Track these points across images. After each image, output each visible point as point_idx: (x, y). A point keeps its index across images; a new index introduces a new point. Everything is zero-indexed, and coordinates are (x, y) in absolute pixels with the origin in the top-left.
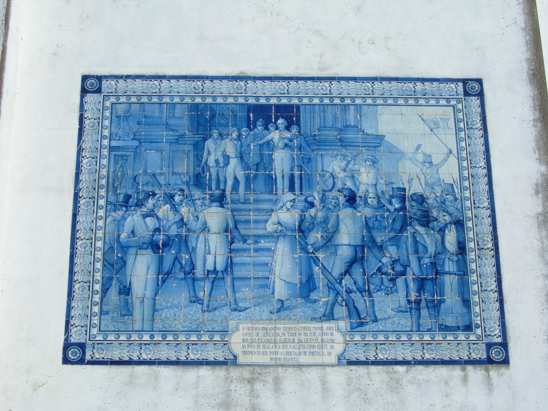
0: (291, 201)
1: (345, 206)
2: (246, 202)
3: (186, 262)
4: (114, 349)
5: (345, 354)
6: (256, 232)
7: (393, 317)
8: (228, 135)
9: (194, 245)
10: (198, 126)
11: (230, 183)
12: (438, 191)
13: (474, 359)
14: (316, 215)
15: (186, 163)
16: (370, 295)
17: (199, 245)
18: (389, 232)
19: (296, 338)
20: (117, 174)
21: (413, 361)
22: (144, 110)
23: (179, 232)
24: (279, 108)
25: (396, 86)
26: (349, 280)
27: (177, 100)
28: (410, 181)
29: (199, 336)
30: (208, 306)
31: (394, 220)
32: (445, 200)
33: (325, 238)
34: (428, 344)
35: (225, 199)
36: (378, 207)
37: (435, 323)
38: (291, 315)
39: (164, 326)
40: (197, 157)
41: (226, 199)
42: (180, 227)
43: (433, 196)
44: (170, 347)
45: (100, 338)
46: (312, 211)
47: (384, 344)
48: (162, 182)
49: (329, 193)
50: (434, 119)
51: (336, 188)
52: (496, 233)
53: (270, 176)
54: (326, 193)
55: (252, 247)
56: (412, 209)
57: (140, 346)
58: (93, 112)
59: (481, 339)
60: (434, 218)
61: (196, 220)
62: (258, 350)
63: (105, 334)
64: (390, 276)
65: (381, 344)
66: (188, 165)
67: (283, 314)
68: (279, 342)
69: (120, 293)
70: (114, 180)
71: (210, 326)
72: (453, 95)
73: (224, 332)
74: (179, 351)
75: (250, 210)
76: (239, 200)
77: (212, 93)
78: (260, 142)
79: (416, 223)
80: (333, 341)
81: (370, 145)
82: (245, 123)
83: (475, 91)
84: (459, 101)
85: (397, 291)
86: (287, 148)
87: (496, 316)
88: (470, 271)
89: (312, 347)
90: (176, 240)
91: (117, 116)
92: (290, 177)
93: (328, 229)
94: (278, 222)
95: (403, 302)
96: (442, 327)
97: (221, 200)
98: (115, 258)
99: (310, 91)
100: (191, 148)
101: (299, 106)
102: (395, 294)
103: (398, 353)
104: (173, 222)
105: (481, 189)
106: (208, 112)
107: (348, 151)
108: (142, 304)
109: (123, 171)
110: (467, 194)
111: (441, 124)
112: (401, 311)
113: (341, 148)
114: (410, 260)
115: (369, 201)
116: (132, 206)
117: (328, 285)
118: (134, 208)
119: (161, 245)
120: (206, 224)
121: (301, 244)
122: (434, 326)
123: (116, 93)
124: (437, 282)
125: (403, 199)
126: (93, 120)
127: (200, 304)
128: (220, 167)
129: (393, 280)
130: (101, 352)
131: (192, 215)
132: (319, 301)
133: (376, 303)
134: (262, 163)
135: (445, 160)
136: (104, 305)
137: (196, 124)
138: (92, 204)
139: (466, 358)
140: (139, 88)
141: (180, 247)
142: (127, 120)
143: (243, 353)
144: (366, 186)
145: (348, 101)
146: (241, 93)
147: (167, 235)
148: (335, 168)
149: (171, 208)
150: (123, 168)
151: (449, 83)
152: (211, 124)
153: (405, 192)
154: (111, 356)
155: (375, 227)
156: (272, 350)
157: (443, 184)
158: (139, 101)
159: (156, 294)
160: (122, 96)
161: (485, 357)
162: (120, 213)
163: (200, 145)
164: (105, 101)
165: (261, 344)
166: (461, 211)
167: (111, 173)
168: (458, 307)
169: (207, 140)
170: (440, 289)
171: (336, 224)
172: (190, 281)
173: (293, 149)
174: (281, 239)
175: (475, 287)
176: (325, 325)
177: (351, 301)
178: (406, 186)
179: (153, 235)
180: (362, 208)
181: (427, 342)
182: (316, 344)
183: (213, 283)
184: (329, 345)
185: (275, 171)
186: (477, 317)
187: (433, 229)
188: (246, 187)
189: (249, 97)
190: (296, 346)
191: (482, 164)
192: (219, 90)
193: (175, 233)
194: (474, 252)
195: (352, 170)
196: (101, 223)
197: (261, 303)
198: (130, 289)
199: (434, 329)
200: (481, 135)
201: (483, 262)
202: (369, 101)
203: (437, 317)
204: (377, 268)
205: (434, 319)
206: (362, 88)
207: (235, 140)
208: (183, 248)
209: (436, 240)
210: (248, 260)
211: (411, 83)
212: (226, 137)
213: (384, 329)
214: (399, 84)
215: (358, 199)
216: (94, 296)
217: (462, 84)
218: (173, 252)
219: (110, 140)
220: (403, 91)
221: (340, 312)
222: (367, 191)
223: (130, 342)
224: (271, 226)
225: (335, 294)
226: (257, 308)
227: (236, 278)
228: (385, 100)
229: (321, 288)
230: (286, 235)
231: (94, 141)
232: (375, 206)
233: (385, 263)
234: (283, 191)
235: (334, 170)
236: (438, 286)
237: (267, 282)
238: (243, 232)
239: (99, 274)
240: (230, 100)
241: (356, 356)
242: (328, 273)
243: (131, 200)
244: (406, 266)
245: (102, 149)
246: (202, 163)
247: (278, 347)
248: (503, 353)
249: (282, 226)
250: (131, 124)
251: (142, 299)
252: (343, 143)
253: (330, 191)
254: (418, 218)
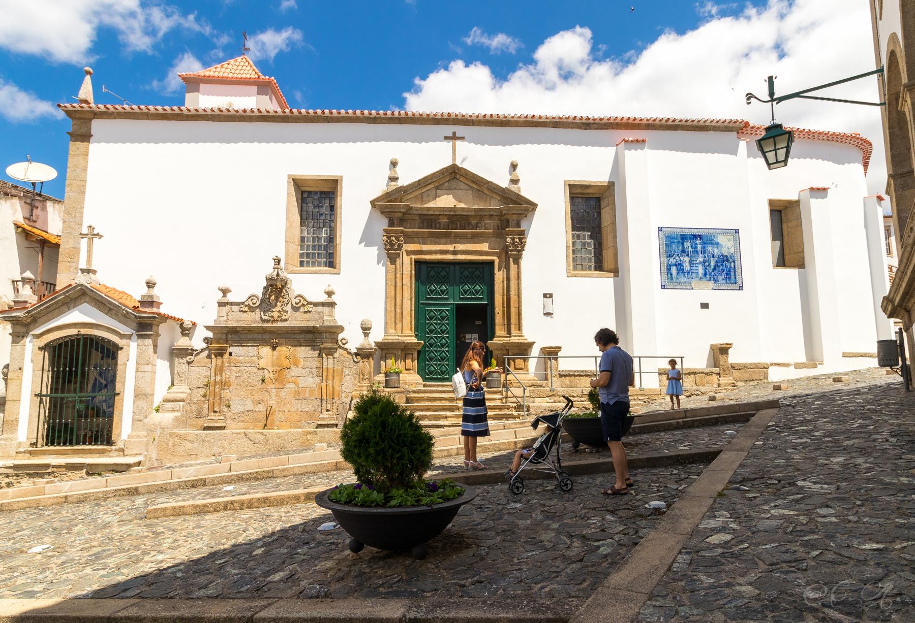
24: (698, 235)
73: (690, 283)
97: (688, 256)
252: (712, 244)
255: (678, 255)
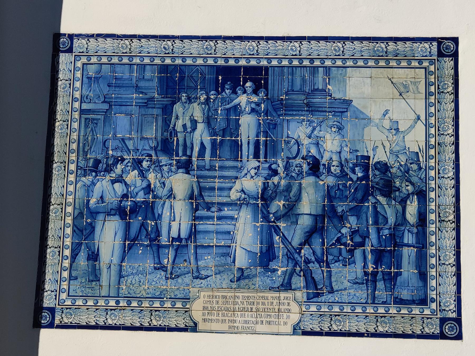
0: (255, 169)
1: (308, 175)
2: (212, 168)
3: (152, 229)
4: (81, 314)
5: (300, 324)
6: (221, 200)
7: (350, 289)
8: (197, 98)
9: (160, 212)
10: (167, 88)
11: (196, 149)
12: (403, 161)
13: (427, 333)
14: (279, 183)
15: (155, 128)
16: (328, 266)
17: (164, 212)
18: (350, 202)
19: (254, 307)
20: (87, 138)
21: (366, 333)
22: (114, 72)
23: (145, 199)
25: (367, 46)
26: (308, 250)
27: (147, 61)
28: (375, 149)
29: (162, 303)
30: (171, 273)
31: (356, 190)
32: (409, 170)
33: (287, 207)
34: (382, 317)
35: (191, 165)
36: (341, 176)
37: (390, 296)
38: (250, 283)
39: (129, 293)
40: (166, 121)
41: (192, 165)
42: (147, 194)
43: (397, 165)
44: (134, 313)
45: (68, 302)
46: (276, 179)
47: (339, 316)
48: (131, 147)
49: (294, 160)
50: (404, 83)
51: (301, 155)
52: (459, 204)
53: (236, 142)
54: (290, 161)
55: (216, 214)
56: (375, 178)
57: (106, 311)
58: (64, 72)
59: (435, 314)
60: (396, 187)
61: (163, 186)
62: (218, 318)
63: (74, 299)
64: (349, 247)
65: (336, 316)
66: (156, 130)
67: (243, 283)
68: (237, 310)
69: (88, 259)
70: (84, 145)
71: (172, 293)
72: (426, 56)
73: (186, 299)
74: (143, 317)
75: (215, 177)
76: (204, 167)
77: (182, 54)
78: (228, 106)
79: (378, 193)
80: (289, 311)
81: (337, 110)
82: (213, 86)
83: (450, 51)
84: (432, 62)
85: (354, 262)
86: (254, 113)
87: (452, 291)
88: (429, 243)
89: (269, 317)
90: (143, 206)
91: (88, 78)
92: (255, 143)
93: (290, 198)
94: (241, 189)
95: (360, 273)
96: (397, 300)
98: (85, 224)
99: (279, 52)
100: (159, 111)
101: (268, 68)
102: (353, 265)
103: (351, 324)
104: (140, 188)
105: (447, 158)
106: (178, 74)
107: (314, 117)
108: (109, 270)
109: (93, 135)
110: (432, 163)
111: (411, 87)
112: (357, 283)
113: (308, 113)
114: (369, 231)
115: (333, 169)
116: (102, 172)
117: (287, 255)
118: (103, 173)
119: (128, 211)
120: (172, 190)
121: (263, 212)
122: (389, 299)
123: (87, 52)
124: (395, 254)
125: (366, 168)
126: (64, 81)
127: (163, 271)
128: (187, 132)
129: (351, 252)
130: (69, 316)
131: (159, 181)
132: (278, 270)
133: (333, 274)
134: (229, 128)
135: (412, 127)
136: (73, 270)
137: (165, 87)
138: (63, 168)
139: (419, 332)
140: (109, 48)
141: (146, 214)
142: (98, 82)
143: (203, 321)
144: (330, 153)
145: (317, 63)
146: (211, 54)
147: (134, 201)
148: (300, 134)
149: (139, 174)
150: (93, 132)
151: (423, 42)
152: (180, 87)
153: (369, 160)
154: (79, 321)
155: (337, 196)
156: (230, 318)
157: (408, 153)
158: (110, 61)
159: (123, 260)
160: (93, 56)
161: (439, 332)
162: (90, 178)
163: (169, 109)
164: (76, 62)
165: (221, 312)
166: (424, 182)
167: (81, 137)
168: (415, 281)
169: (176, 103)
170: (398, 261)
171: (299, 193)
172: (155, 248)
173: (260, 114)
174: (244, 207)
175: (433, 261)
176: (283, 295)
177: (309, 271)
178: (371, 154)
179: (121, 201)
180: (325, 176)
181: (381, 315)
182: (273, 314)
183: (176, 250)
184: (285, 314)
185: (241, 137)
186: (432, 291)
187: (395, 200)
188: (212, 154)
189: (218, 59)
190: (254, 315)
191: (451, 131)
192: (189, 51)
193: (142, 200)
194: (435, 224)
195: (317, 136)
196: (71, 188)
197: (222, 272)
198: (98, 255)
199: (388, 301)
200: (452, 100)
201: (443, 235)
202: (339, 63)
203: (392, 289)
204: (336, 238)
205: (389, 292)
206: (333, 49)
207: (203, 103)
208: (150, 215)
209: (397, 210)
210: (211, 228)
211: (383, 43)
212: (194, 101)
213: (340, 301)
214: (370, 44)
215: (322, 167)
216: (64, 261)
217: (437, 44)
218: (140, 218)
219: (81, 103)
220: (375, 51)
221: (298, 282)
222: (331, 158)
223: (97, 308)
224: (235, 194)
225: (293, 264)
226: (218, 276)
227: (199, 246)
228: (355, 62)
229: (281, 258)
230: (249, 203)
231: (65, 103)
232: (337, 175)
233: (344, 234)
234: (248, 158)
235: (299, 137)
236: (395, 258)
237: (228, 250)
238: (207, 199)
239: (68, 239)
240: (200, 61)
241: (311, 327)
242: (287, 243)
243: (100, 165)
244: (365, 237)
245: (73, 112)
246: (170, 128)
247: (236, 316)
248: (457, 329)
249: (245, 194)
250: (102, 86)
251: (109, 265)
253: (295, 158)
254: (380, 188)
255: (137, 164)
